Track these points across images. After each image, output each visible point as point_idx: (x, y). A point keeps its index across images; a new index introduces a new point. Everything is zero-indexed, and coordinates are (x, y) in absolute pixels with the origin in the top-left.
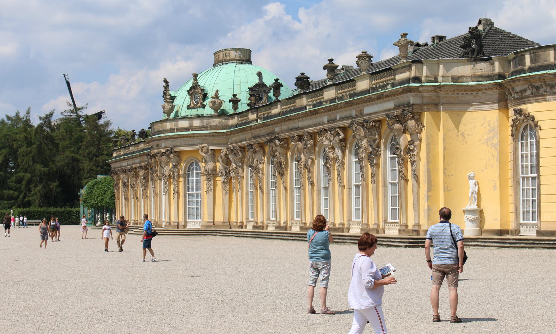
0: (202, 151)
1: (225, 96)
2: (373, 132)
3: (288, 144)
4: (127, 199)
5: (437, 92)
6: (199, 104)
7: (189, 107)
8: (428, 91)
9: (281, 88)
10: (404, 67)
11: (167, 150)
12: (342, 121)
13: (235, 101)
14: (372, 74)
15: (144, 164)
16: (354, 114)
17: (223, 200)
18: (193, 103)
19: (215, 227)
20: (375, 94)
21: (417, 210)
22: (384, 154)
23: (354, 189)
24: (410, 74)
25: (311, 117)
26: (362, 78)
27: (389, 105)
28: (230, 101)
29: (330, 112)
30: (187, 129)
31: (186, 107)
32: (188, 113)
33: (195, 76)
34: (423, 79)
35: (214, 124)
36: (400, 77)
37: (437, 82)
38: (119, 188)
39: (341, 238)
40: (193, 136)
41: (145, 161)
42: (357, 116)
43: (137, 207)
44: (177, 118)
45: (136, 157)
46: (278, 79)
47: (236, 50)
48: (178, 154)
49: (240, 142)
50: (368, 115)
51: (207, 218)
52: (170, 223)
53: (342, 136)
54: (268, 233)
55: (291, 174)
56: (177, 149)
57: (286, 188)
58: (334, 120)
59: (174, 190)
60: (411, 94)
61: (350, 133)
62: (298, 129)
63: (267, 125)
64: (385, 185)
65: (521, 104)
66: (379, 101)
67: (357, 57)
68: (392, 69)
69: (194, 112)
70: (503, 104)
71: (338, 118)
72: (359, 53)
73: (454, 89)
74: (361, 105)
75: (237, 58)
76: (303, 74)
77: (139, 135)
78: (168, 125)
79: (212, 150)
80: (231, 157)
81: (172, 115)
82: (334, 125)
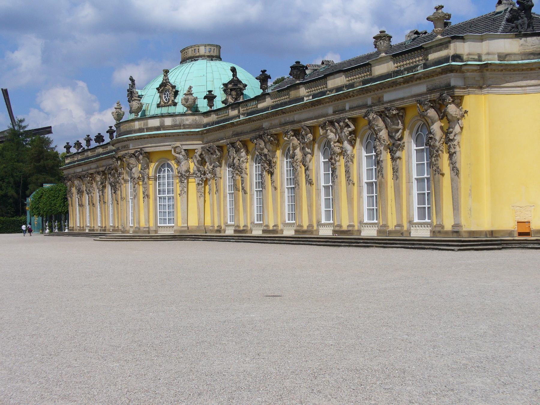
1: (199, 93)
2: (396, 122)
3: (278, 141)
4: (81, 205)
5: (482, 72)
6: (170, 102)
7: (159, 106)
8: (473, 71)
9: (269, 80)
10: (441, 44)
11: (136, 152)
12: (353, 111)
13: (210, 97)
14: (394, 56)
15: (101, 169)
16: (369, 102)
17: (198, 202)
18: (163, 101)
19: (189, 232)
20: (402, 77)
22: (408, 146)
23: (365, 187)
25: (311, 108)
26: (381, 61)
27: (421, 88)
28: (205, 98)
29: (336, 102)
30: (158, 129)
31: (156, 106)
32: (158, 111)
33: (166, 72)
34: (465, 57)
35: (187, 123)
36: (432, 56)
37: (481, 61)
38: (72, 194)
39: (361, 241)
40: (166, 135)
41: (103, 166)
42: (373, 105)
43: (93, 213)
44: (144, 117)
45: (92, 162)
46: (265, 71)
48: (148, 155)
49: (218, 140)
50: (390, 102)
51: (180, 223)
52: (139, 228)
54: (317, 238)
55: (282, 173)
56: (148, 150)
58: (343, 111)
59: (144, 193)
60: (452, 74)
61: (363, 123)
62: (293, 122)
63: (254, 121)
64: (409, 181)
66: (406, 85)
67: (374, 38)
68: (423, 48)
69: (164, 110)
71: (347, 108)
72: (293, 63)
73: (502, 68)
74: (380, 91)
76: (298, 62)
77: (95, 140)
78: (137, 125)
79: (185, 150)
82: (342, 116)
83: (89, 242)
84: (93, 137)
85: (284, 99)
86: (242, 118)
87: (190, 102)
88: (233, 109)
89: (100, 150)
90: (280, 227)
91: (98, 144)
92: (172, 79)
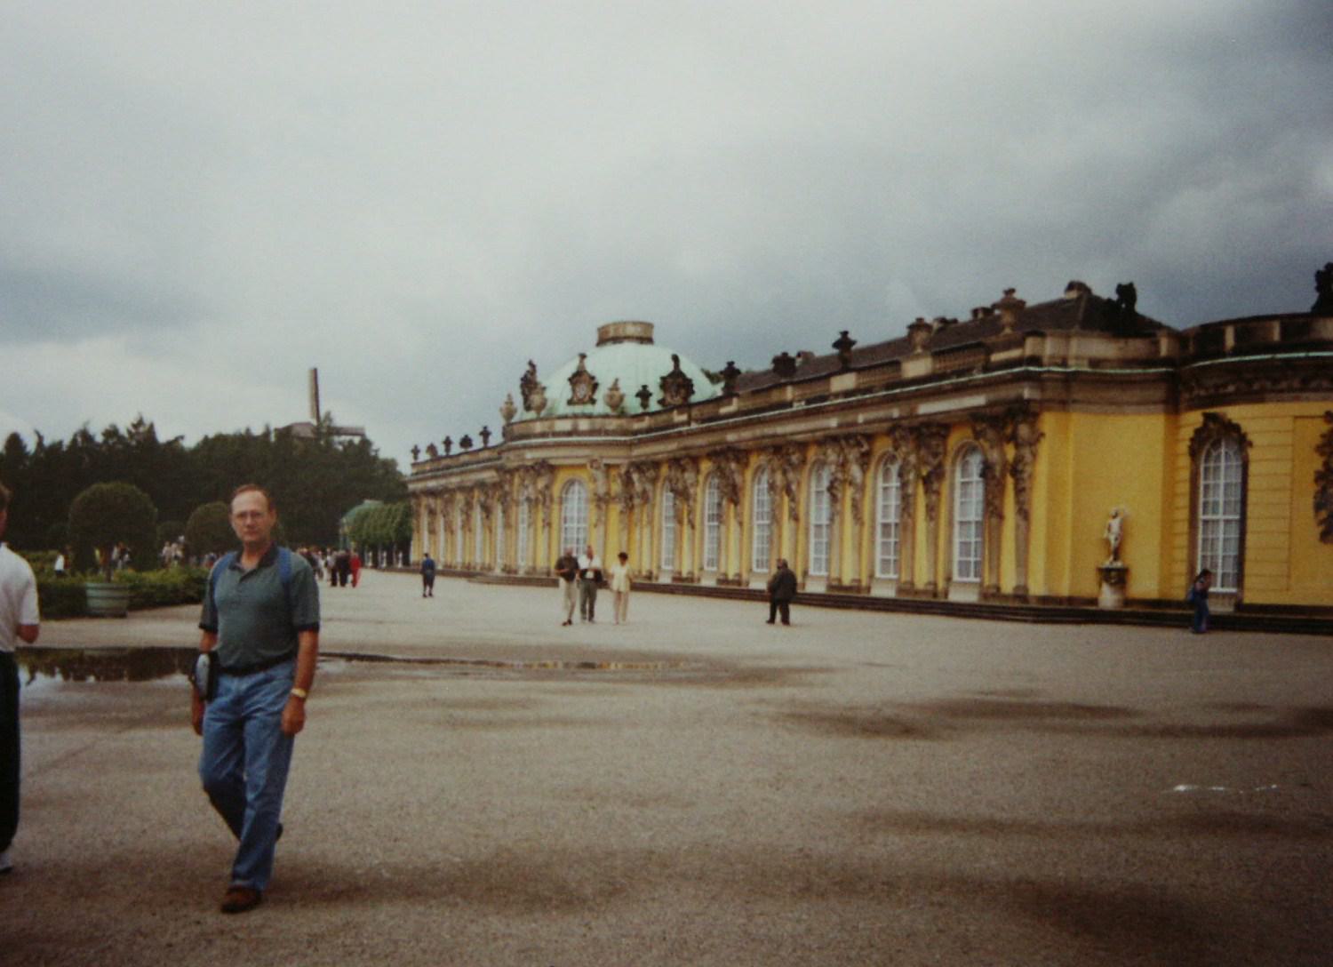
0: (592, 467)
1: (629, 390)
4: (432, 532)
7: (570, 402)
11: (536, 464)
21: (1022, 562)
23: (879, 530)
24: (1024, 352)
30: (569, 434)
33: (583, 356)
34: (1046, 360)
36: (997, 357)
47: (635, 323)
53: (865, 448)
57: (741, 524)
59: (544, 521)
65: (1212, 405)
69: (578, 409)
70: (1173, 406)
75: (637, 334)
80: (635, 477)
81: (543, 413)
82: (852, 430)
83: (462, 582)
84: (456, 440)
85: (760, 401)
86: (694, 426)
87: (616, 399)
88: (681, 413)
89: (466, 458)
90: (745, 576)
91: (462, 450)
92: (590, 367)
